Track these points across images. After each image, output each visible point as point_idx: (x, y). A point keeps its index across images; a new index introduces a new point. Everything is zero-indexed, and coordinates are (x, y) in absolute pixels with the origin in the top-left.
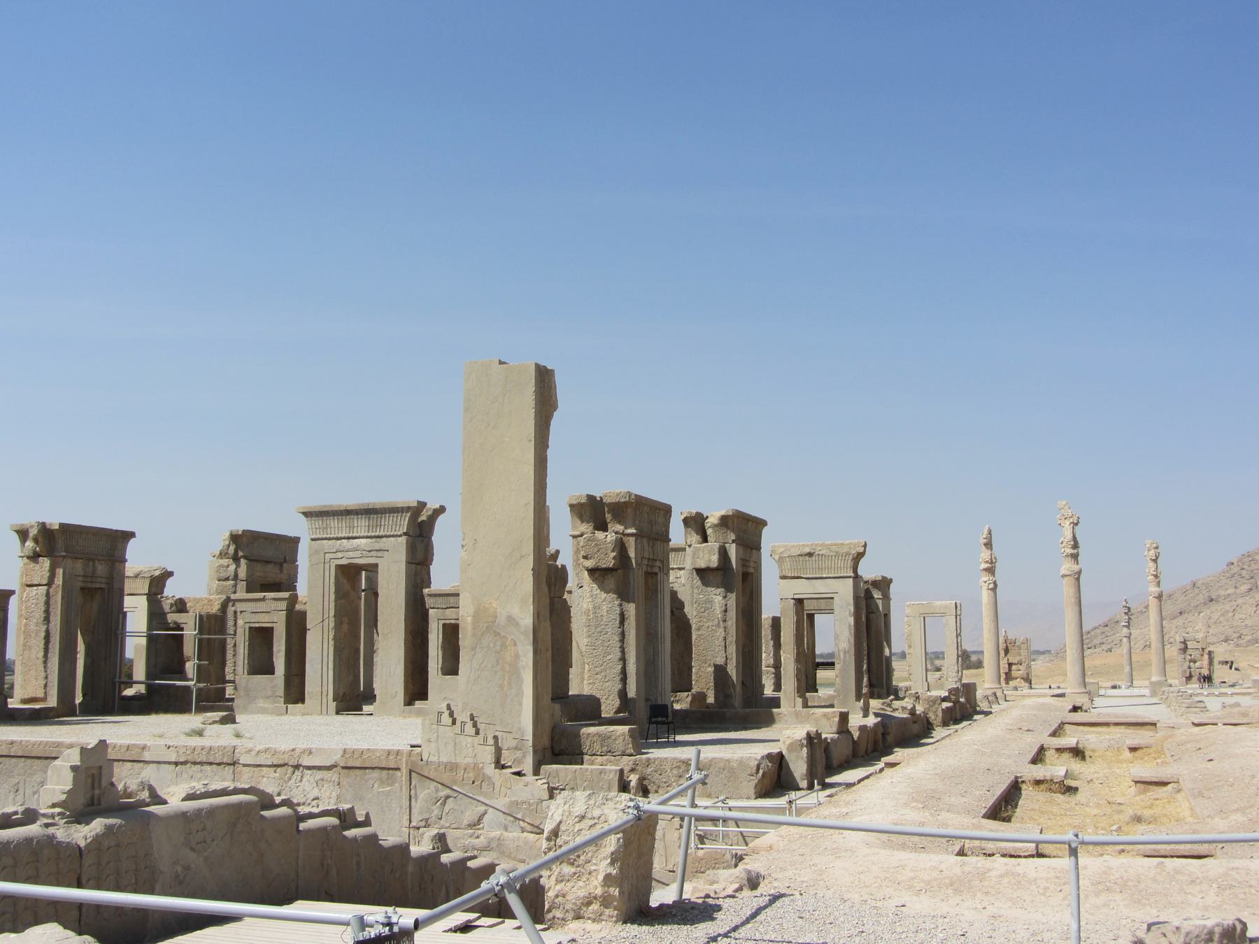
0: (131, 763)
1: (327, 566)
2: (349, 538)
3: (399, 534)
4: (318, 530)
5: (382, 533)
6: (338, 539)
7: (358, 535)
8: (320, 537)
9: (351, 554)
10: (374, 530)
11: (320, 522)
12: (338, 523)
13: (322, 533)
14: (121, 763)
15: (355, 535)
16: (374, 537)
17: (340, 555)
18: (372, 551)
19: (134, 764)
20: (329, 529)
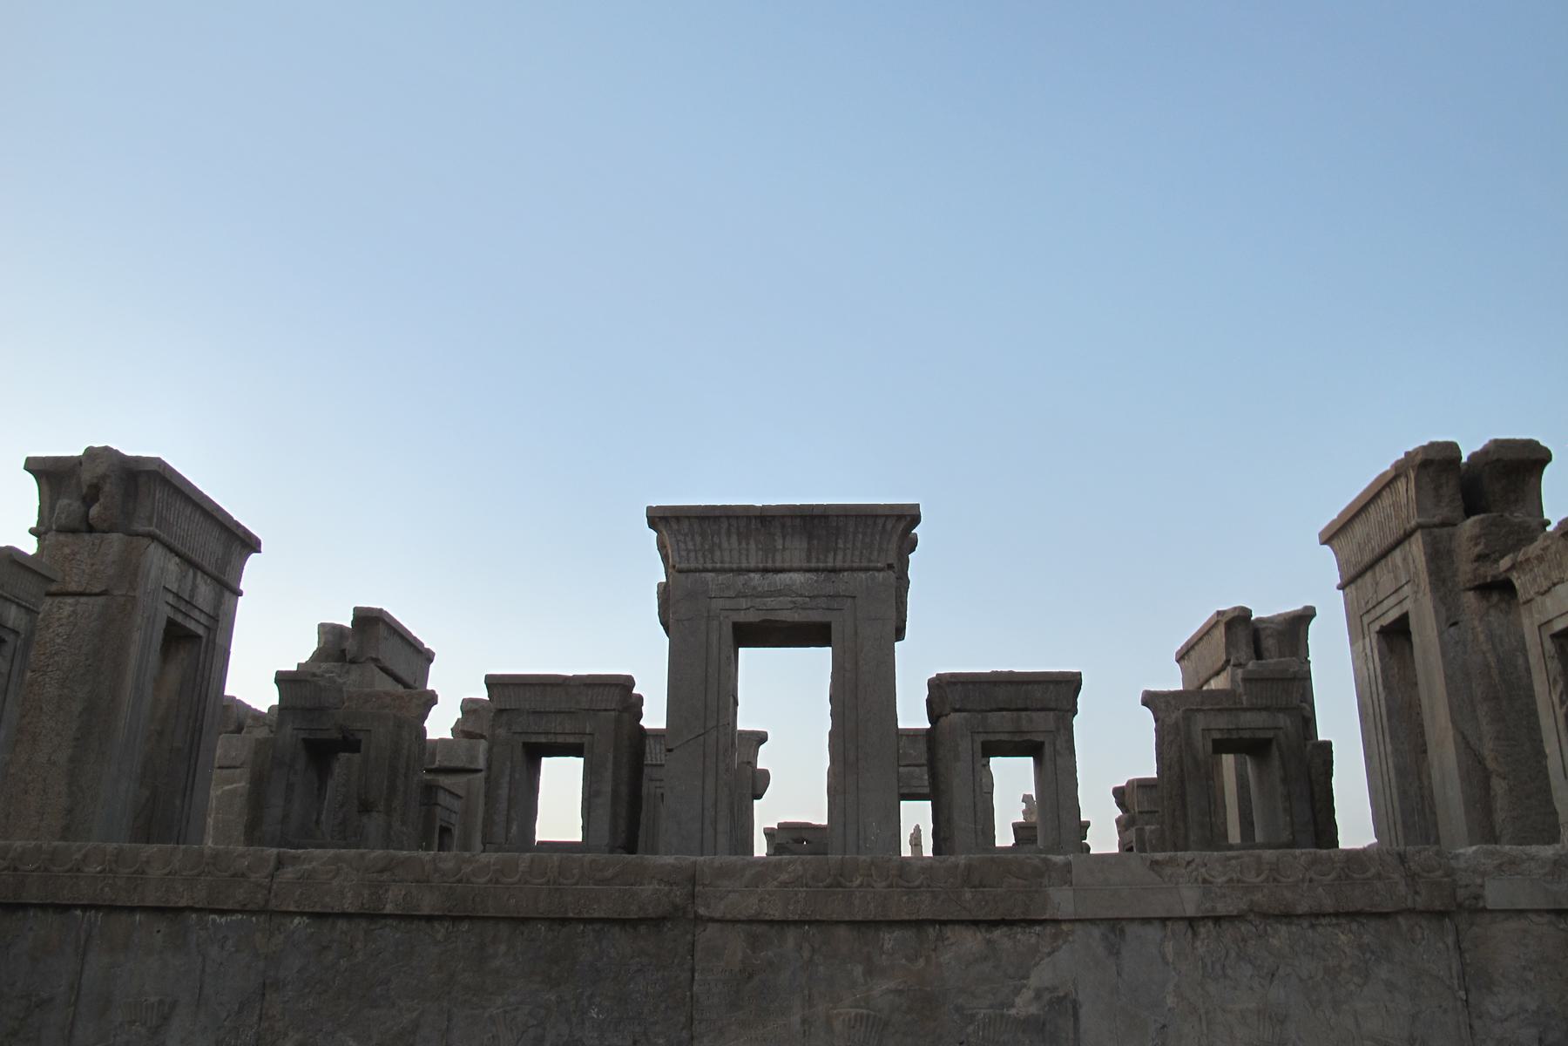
1: (715, 623)
4: (692, 555)
5: (839, 564)
6: (740, 571)
7: (786, 565)
9: (771, 602)
10: (822, 557)
11: (698, 539)
12: (740, 543)
13: (701, 561)
14: (932, 932)
15: (778, 564)
16: (824, 570)
17: (743, 603)
19: (997, 933)
20: (718, 553)
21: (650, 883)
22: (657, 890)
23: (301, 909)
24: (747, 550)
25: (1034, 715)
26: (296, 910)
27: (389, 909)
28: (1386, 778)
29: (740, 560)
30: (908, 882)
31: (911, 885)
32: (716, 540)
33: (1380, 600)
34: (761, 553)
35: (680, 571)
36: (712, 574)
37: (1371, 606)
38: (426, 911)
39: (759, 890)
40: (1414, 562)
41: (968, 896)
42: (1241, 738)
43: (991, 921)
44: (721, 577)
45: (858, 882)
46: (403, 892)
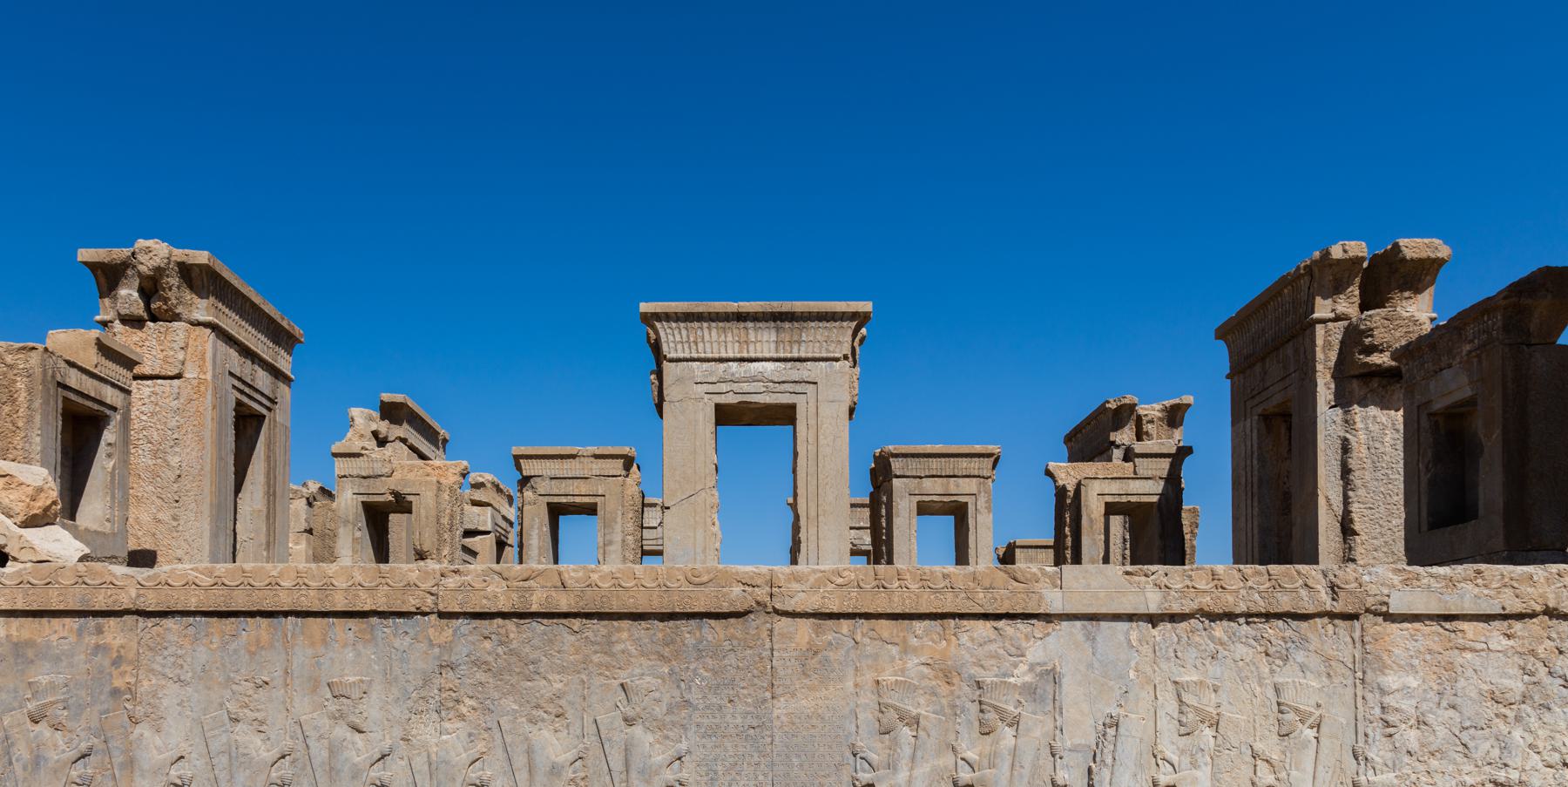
0: (989, 624)
2: (742, 360)
3: (837, 355)
4: (679, 346)
5: (803, 355)
7: (759, 355)
8: (687, 355)
10: (788, 348)
11: (684, 332)
12: (719, 336)
13: (687, 350)
15: (753, 355)
17: (724, 387)
18: (784, 382)
19: (1002, 624)
20: (701, 345)
21: (737, 586)
22: (744, 591)
23: (464, 610)
24: (725, 342)
25: (960, 480)
26: (460, 610)
27: (534, 608)
28: (1250, 534)
29: (719, 350)
30: (935, 584)
31: (937, 587)
32: (699, 333)
33: (1266, 387)
34: (737, 344)
35: (671, 360)
36: (698, 363)
37: (1256, 392)
38: (565, 609)
39: (821, 590)
40: (1305, 352)
41: (981, 595)
42: (1129, 502)
43: (998, 614)
44: (705, 365)
45: (897, 585)
46: (545, 596)
